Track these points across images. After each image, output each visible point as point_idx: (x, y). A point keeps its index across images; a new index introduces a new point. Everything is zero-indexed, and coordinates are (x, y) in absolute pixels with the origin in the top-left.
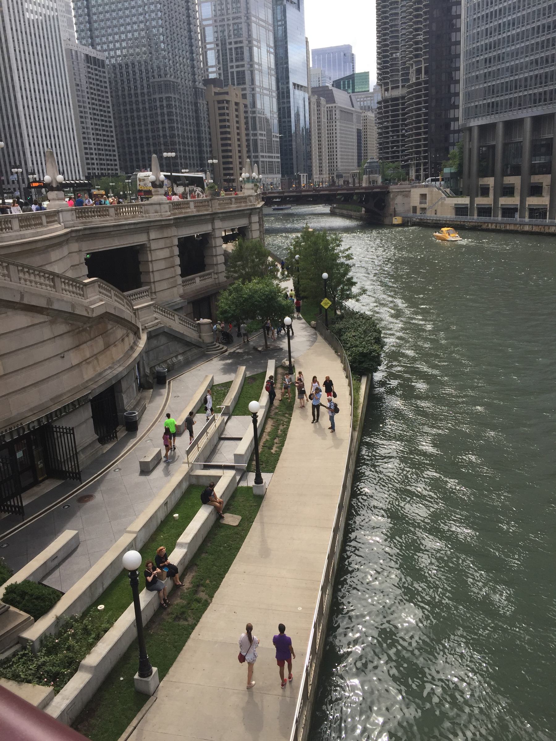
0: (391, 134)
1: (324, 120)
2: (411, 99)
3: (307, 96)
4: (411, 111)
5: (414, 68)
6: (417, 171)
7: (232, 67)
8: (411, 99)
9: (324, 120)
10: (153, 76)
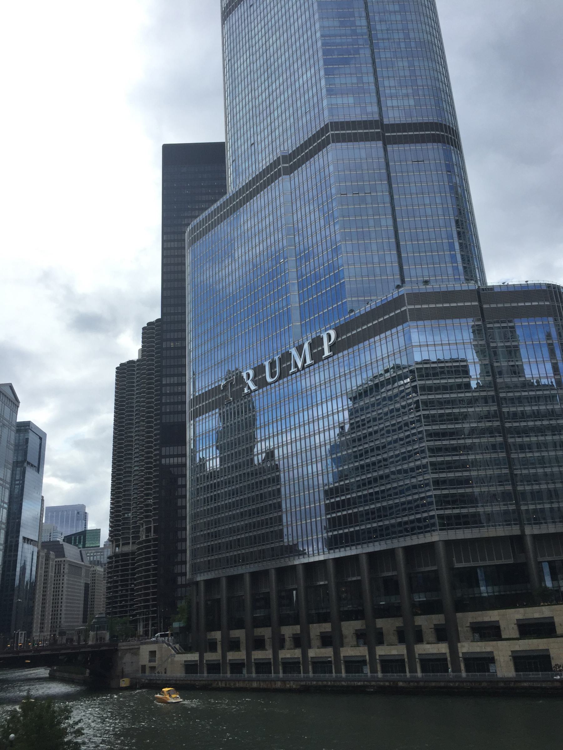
0: (120, 588)
1: (51, 574)
2: (141, 554)
3: (36, 549)
4: (141, 566)
5: (144, 527)
6: (146, 626)
8: (141, 554)
9: (51, 574)
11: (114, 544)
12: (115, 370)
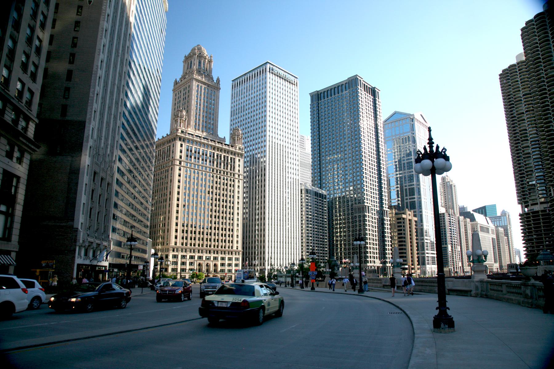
7: (407, 199)
10: (356, 203)
11: (524, 205)
12: (499, 77)
